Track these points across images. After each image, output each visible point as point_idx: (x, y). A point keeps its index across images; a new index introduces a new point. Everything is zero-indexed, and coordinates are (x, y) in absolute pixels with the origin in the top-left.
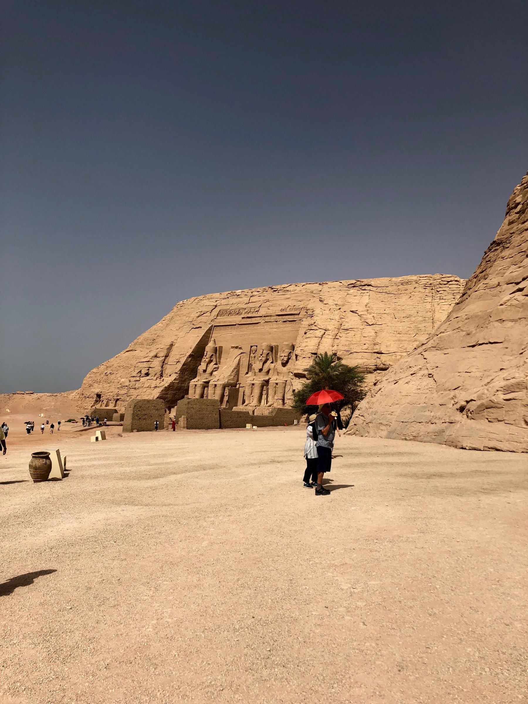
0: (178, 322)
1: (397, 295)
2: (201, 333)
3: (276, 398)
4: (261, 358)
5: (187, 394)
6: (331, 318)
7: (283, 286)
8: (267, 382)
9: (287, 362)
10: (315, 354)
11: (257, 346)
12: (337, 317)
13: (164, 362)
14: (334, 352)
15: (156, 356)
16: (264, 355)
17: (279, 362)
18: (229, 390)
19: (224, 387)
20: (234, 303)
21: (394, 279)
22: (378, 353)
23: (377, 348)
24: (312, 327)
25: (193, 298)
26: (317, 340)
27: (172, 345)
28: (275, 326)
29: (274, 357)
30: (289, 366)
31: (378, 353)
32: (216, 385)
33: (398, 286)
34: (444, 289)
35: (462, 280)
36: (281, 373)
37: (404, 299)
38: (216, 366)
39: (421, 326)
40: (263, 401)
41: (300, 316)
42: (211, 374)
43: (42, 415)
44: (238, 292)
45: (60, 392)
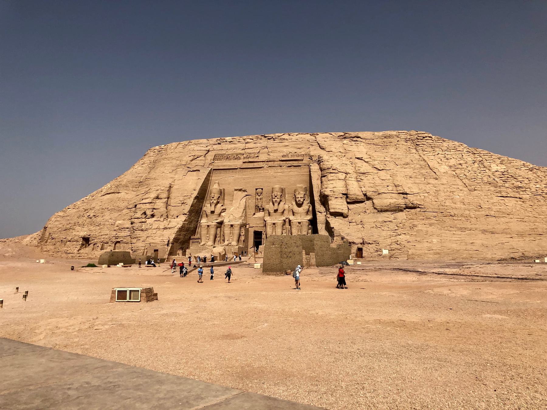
0: (167, 165)
1: (385, 146)
11: (262, 189)
15: (157, 198)
20: (226, 148)
21: (376, 133)
22: (403, 194)
23: (400, 189)
25: (174, 144)
28: (279, 171)
31: (403, 194)
33: (382, 139)
35: (433, 137)
36: (297, 213)
37: (392, 150)
41: (304, 162)
44: (228, 139)
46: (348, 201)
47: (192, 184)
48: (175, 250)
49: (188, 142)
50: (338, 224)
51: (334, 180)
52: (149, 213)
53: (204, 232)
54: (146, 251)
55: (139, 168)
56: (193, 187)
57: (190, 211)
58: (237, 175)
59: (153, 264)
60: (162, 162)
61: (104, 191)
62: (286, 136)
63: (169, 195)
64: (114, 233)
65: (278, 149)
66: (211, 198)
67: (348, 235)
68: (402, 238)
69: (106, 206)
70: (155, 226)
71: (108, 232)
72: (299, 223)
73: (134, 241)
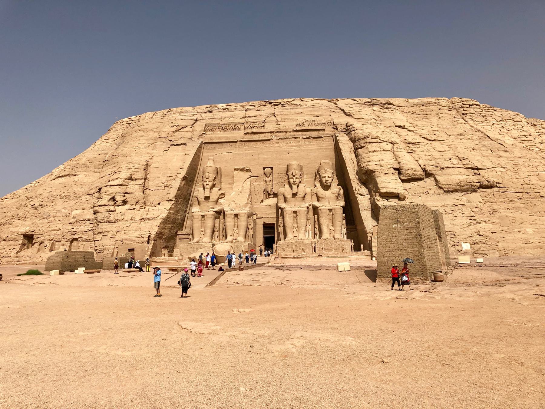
0: (142, 138)
11: (272, 168)
15: (130, 178)
21: (410, 100)
22: (472, 168)
25: (149, 114)
28: (293, 144)
31: (472, 168)
33: (420, 107)
37: (434, 120)
41: (326, 132)
42: (217, 202)
44: (221, 106)
46: (402, 178)
47: (178, 161)
48: (158, 249)
49: (168, 110)
51: (377, 151)
52: (119, 198)
53: (197, 224)
54: (116, 251)
55: (103, 144)
56: (179, 164)
58: (236, 150)
59: (137, 268)
60: (134, 134)
61: (55, 174)
62: (298, 102)
63: (146, 175)
64: (70, 227)
65: (290, 117)
66: (205, 180)
68: (484, 227)
69: (58, 192)
70: (128, 216)
71: (60, 226)
72: (330, 210)
73: (98, 237)
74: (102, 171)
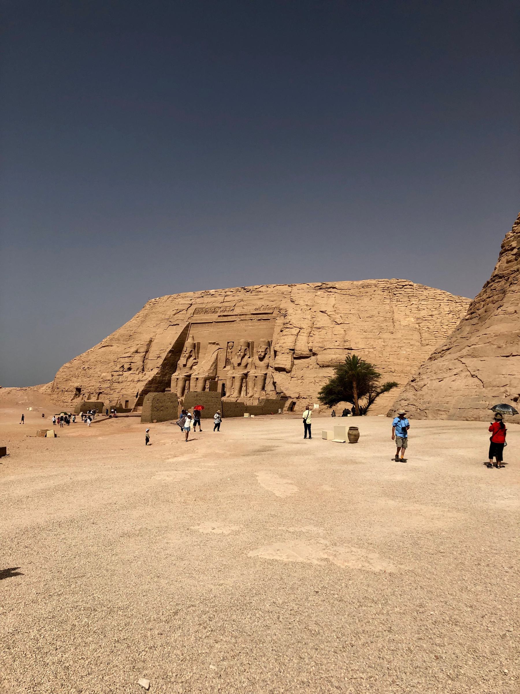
0: (154, 319)
1: (359, 297)
2: (180, 330)
3: (255, 389)
4: (239, 354)
5: (169, 386)
6: (304, 317)
7: (255, 287)
8: (246, 375)
9: (264, 357)
10: (293, 350)
12: (309, 317)
13: (144, 358)
14: (310, 348)
15: (137, 352)
16: (243, 351)
17: (256, 357)
18: (210, 383)
19: (205, 380)
20: (208, 302)
21: (355, 283)
22: (348, 349)
24: (286, 326)
25: (166, 297)
26: (293, 338)
27: (151, 341)
28: (250, 324)
29: (251, 352)
30: (266, 360)
31: (348, 349)
32: (197, 379)
33: (360, 289)
34: (400, 292)
35: (415, 285)
37: (365, 301)
38: (195, 361)
39: (384, 325)
40: (242, 393)
41: (273, 315)
43: (31, 409)
44: (212, 291)
45: (29, 386)
46: (295, 356)
47: (168, 339)
50: (281, 379)
54: (119, 401)
57: (162, 365)
62: (263, 289)
67: (287, 389)
70: (130, 379)
73: (112, 392)
74: (127, 344)
